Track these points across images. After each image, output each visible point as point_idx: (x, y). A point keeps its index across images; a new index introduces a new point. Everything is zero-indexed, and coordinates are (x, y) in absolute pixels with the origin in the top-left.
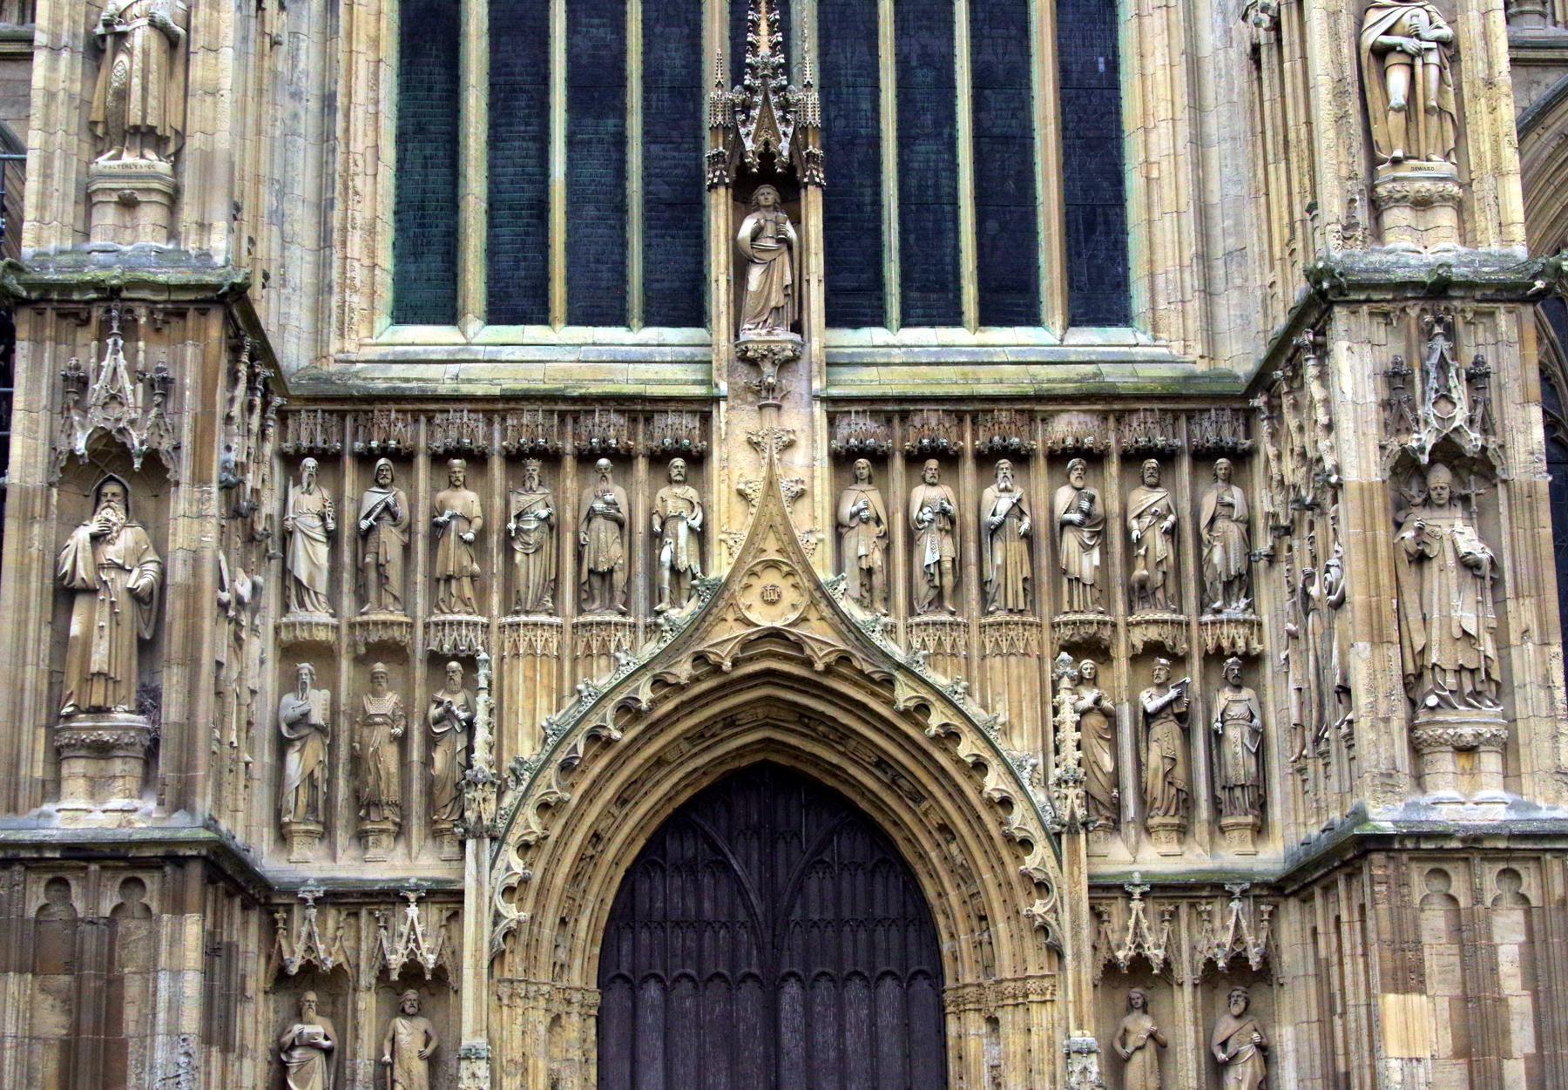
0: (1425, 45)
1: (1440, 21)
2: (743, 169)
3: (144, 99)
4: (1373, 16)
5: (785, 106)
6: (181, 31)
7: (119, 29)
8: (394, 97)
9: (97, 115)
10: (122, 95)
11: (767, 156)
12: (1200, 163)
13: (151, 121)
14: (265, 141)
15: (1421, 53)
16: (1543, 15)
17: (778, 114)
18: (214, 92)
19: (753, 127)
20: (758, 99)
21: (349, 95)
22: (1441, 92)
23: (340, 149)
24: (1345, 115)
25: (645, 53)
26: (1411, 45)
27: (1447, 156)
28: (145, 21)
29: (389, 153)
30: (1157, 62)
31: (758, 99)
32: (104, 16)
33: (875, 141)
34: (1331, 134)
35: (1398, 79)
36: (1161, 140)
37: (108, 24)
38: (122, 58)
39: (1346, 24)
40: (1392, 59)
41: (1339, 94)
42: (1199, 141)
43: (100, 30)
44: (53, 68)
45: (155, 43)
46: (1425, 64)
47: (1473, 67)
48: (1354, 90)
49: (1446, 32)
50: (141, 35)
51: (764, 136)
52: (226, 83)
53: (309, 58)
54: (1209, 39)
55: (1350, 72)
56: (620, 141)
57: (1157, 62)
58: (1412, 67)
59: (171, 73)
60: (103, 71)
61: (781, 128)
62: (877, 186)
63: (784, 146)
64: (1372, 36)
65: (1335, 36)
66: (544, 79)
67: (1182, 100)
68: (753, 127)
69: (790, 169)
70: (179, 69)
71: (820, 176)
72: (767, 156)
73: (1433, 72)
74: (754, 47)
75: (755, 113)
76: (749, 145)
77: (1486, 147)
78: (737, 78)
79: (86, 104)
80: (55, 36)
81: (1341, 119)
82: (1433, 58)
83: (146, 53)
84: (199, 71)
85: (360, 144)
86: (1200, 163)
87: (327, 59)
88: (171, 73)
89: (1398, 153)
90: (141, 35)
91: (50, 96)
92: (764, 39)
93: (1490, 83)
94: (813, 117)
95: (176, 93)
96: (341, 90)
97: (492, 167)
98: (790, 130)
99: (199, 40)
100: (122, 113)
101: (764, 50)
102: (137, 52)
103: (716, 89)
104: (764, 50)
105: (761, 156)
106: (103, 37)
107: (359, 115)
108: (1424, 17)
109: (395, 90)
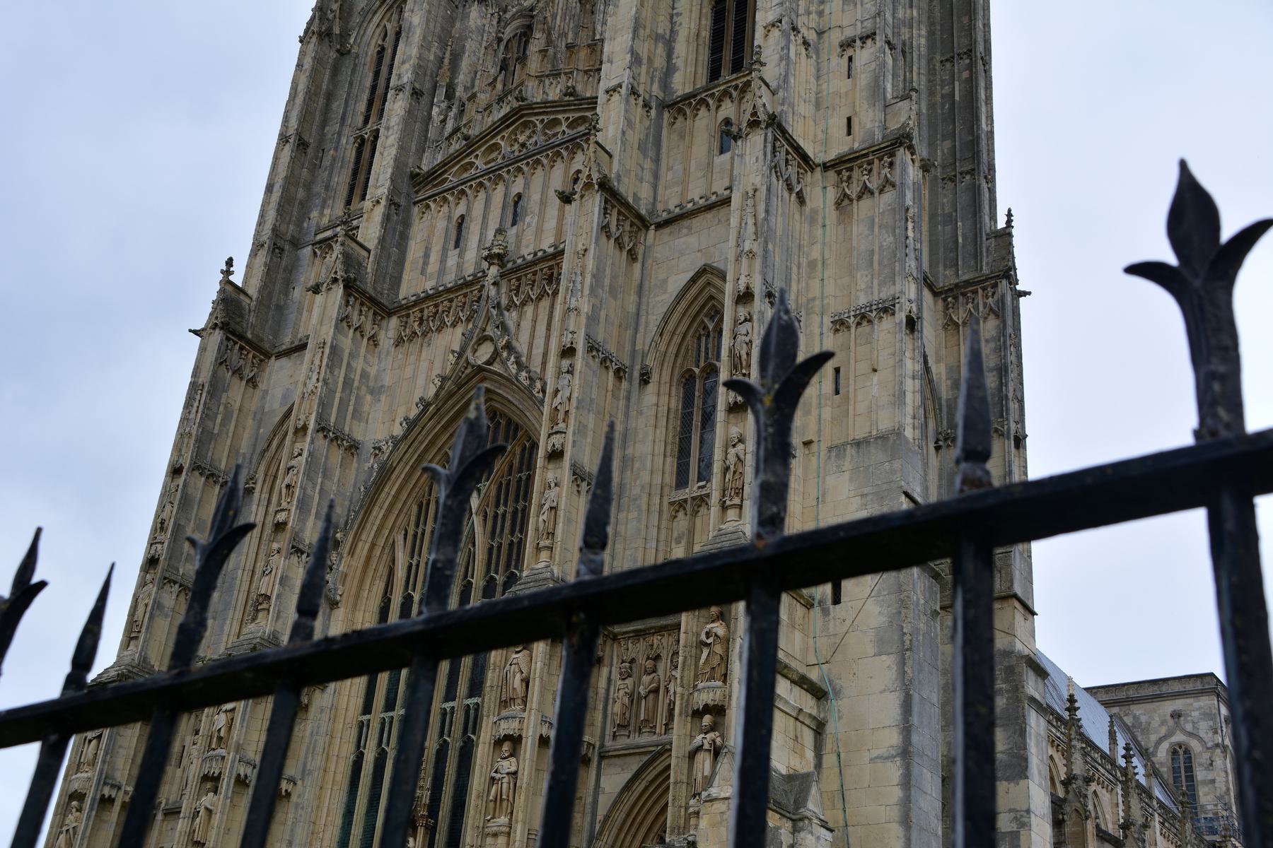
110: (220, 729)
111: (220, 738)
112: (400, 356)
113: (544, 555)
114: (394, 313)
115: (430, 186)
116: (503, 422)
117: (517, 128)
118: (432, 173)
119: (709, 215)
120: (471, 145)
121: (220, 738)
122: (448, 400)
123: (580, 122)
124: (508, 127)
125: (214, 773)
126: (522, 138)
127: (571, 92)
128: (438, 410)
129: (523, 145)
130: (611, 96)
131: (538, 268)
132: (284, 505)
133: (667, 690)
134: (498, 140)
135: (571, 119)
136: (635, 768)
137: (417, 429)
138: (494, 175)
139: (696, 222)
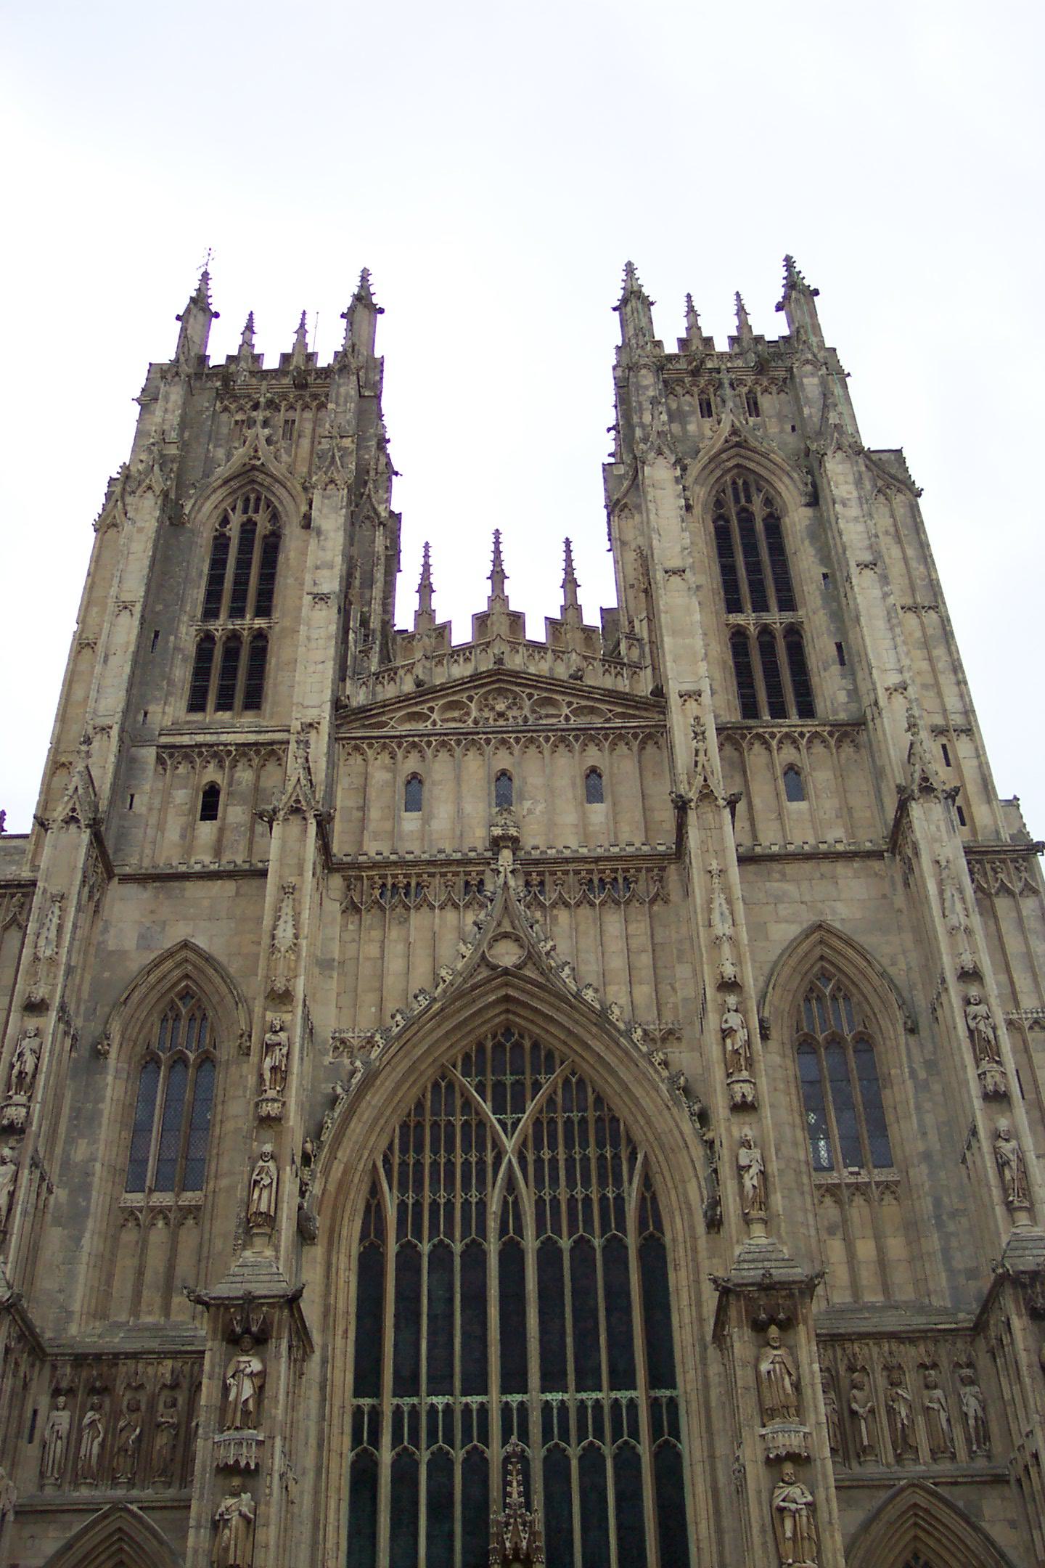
0: (800, 1506)
1: (807, 1493)
2: (505, 1556)
3: (235, 1551)
4: (777, 1492)
5: (525, 1525)
6: (252, 1516)
7: (226, 1517)
8: (347, 1517)
9: (214, 1558)
10: (226, 1549)
11: (516, 1549)
12: (720, 1542)
13: (238, 1562)
14: (287, 1554)
15: (798, 1510)
16: (877, 1462)
17: (521, 1528)
18: (267, 1546)
19: (509, 1535)
20: (512, 1521)
21: (326, 1518)
22: (809, 1528)
23: (321, 1547)
24: (766, 1542)
25: (463, 1490)
26: (793, 1506)
27: (813, 1561)
28: (237, 1513)
29: (344, 1545)
30: (700, 1488)
31: (512, 1521)
32: (220, 1511)
33: (571, 1531)
34: (760, 1552)
35: (788, 1524)
36: (703, 1526)
37: (221, 1515)
38: (227, 1531)
39: (765, 1496)
40: (786, 1513)
41: (763, 1531)
42: (719, 1531)
43: (217, 1517)
44: (197, 1536)
45: (242, 1525)
46: (800, 1516)
47: (823, 1515)
48: (769, 1529)
49: (810, 1498)
50: (235, 1519)
51: (515, 1540)
52: (272, 1542)
53: (307, 1500)
54: (722, 1480)
55: (768, 1520)
56: (451, 1535)
57: (700, 1488)
58: (794, 1517)
59: (247, 1537)
60: (219, 1535)
61: (522, 1535)
62: (572, 1555)
63: (524, 1543)
64: (778, 1502)
65: (760, 1503)
66: (416, 1503)
67: (711, 1511)
68: (509, 1535)
69: (528, 1555)
70: (251, 1533)
71: (543, 1557)
72: (516, 1549)
73: (804, 1519)
74: (510, 1494)
75: (510, 1528)
76: (508, 1544)
77: (830, 1556)
78: (505, 1505)
79: (211, 1551)
80: (199, 1521)
81: (765, 1543)
82: (804, 1513)
83: (237, 1529)
84: (261, 1536)
85: (330, 1544)
86: (720, 1542)
87: (316, 1503)
88: (247, 1537)
89: (790, 1561)
90: (235, 1519)
91: (196, 1551)
92: (515, 1489)
93: (830, 1523)
94: (539, 1527)
95: (249, 1546)
96: (322, 1517)
97: (392, 1549)
98: (527, 1536)
99: (261, 1521)
100: (226, 1559)
101: (515, 1495)
102: (233, 1528)
103: (496, 1515)
104: (515, 1495)
105: (514, 1550)
106: (219, 1521)
107: (330, 1529)
108: (798, 1491)
109: (347, 1512)
110: (247, 1400)
111: (246, 1413)
112: (351, 927)
113: (758, 1229)
114: (337, 870)
115: (357, 724)
116: (527, 1044)
117: (489, 692)
118: (363, 709)
119: (808, 866)
120: (424, 691)
121: (246, 1413)
122: (453, 1002)
123: (585, 711)
124: (476, 687)
125: (248, 1464)
126: (500, 707)
127: (577, 677)
128: (442, 1010)
129: (501, 715)
130: (685, 701)
131: (571, 867)
132: (271, 1094)
133: (891, 1412)
134: (463, 697)
135: (575, 706)
136: (876, 1503)
137: (415, 1027)
138: (468, 740)
139: (791, 869)
